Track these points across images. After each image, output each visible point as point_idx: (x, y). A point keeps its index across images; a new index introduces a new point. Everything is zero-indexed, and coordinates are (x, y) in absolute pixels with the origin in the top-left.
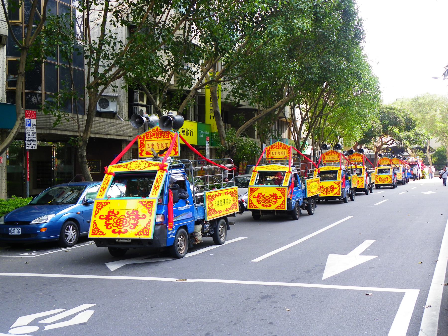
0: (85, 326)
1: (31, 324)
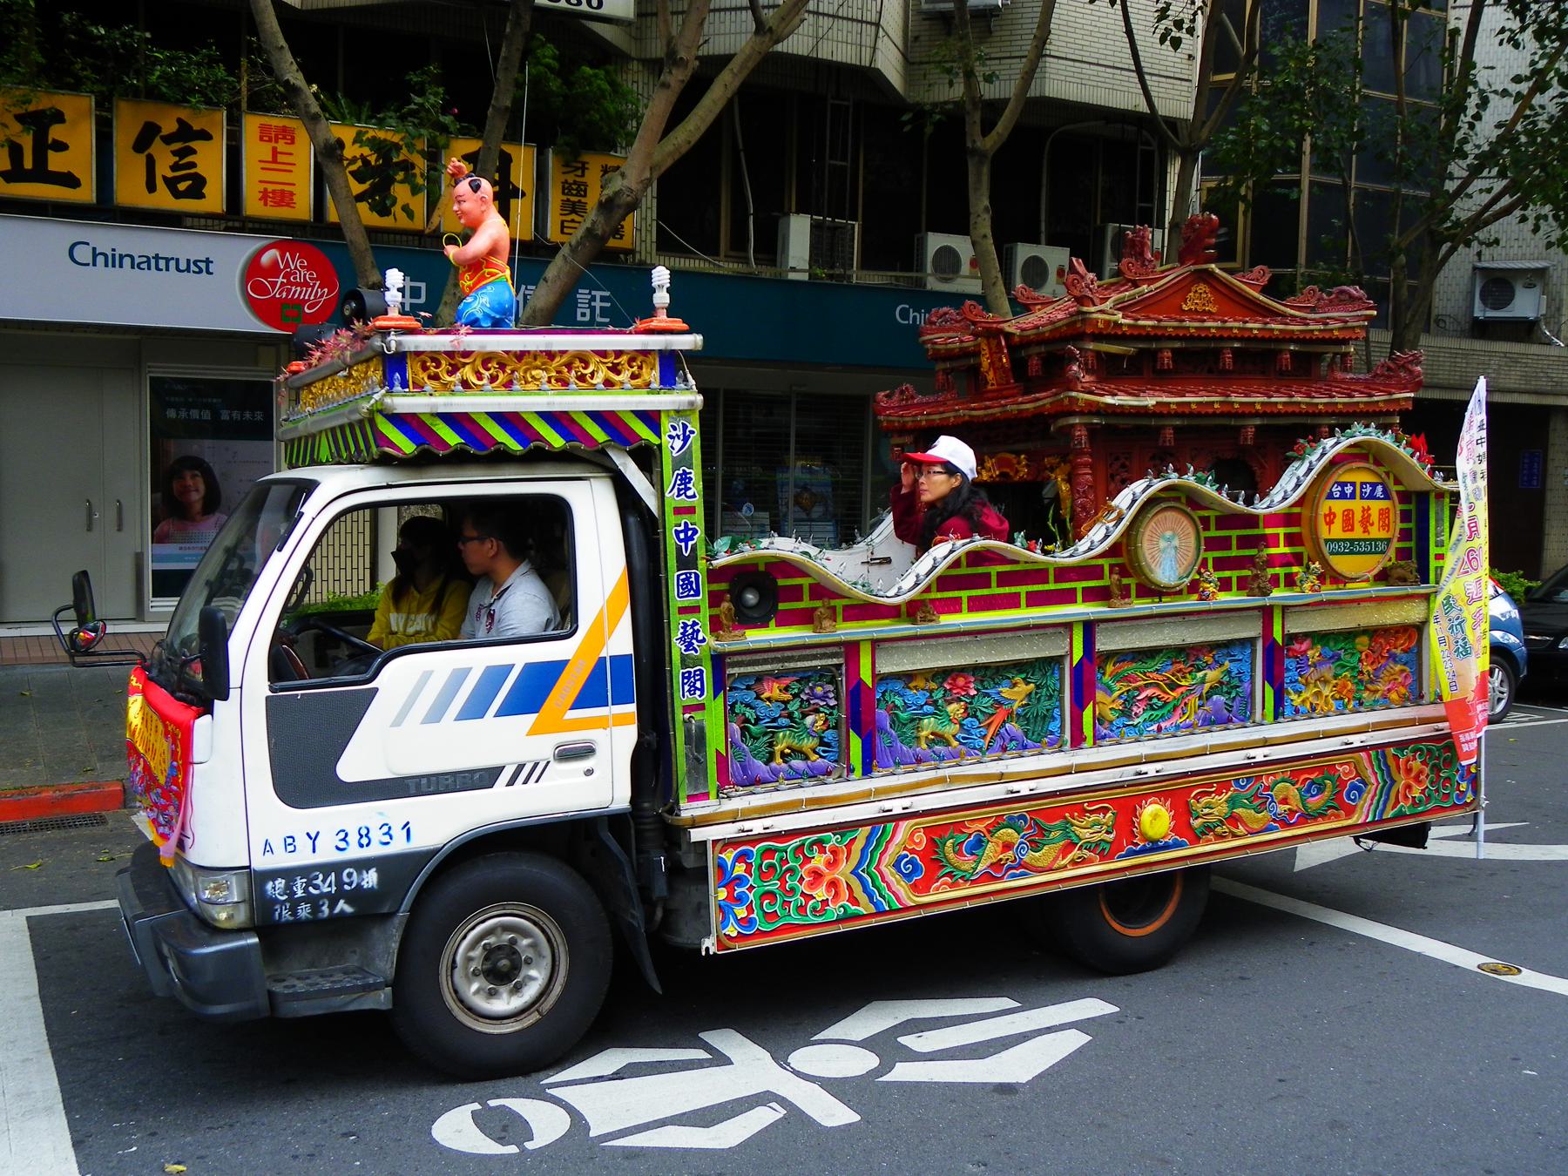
0: (1006, 1100)
1: (867, 1044)
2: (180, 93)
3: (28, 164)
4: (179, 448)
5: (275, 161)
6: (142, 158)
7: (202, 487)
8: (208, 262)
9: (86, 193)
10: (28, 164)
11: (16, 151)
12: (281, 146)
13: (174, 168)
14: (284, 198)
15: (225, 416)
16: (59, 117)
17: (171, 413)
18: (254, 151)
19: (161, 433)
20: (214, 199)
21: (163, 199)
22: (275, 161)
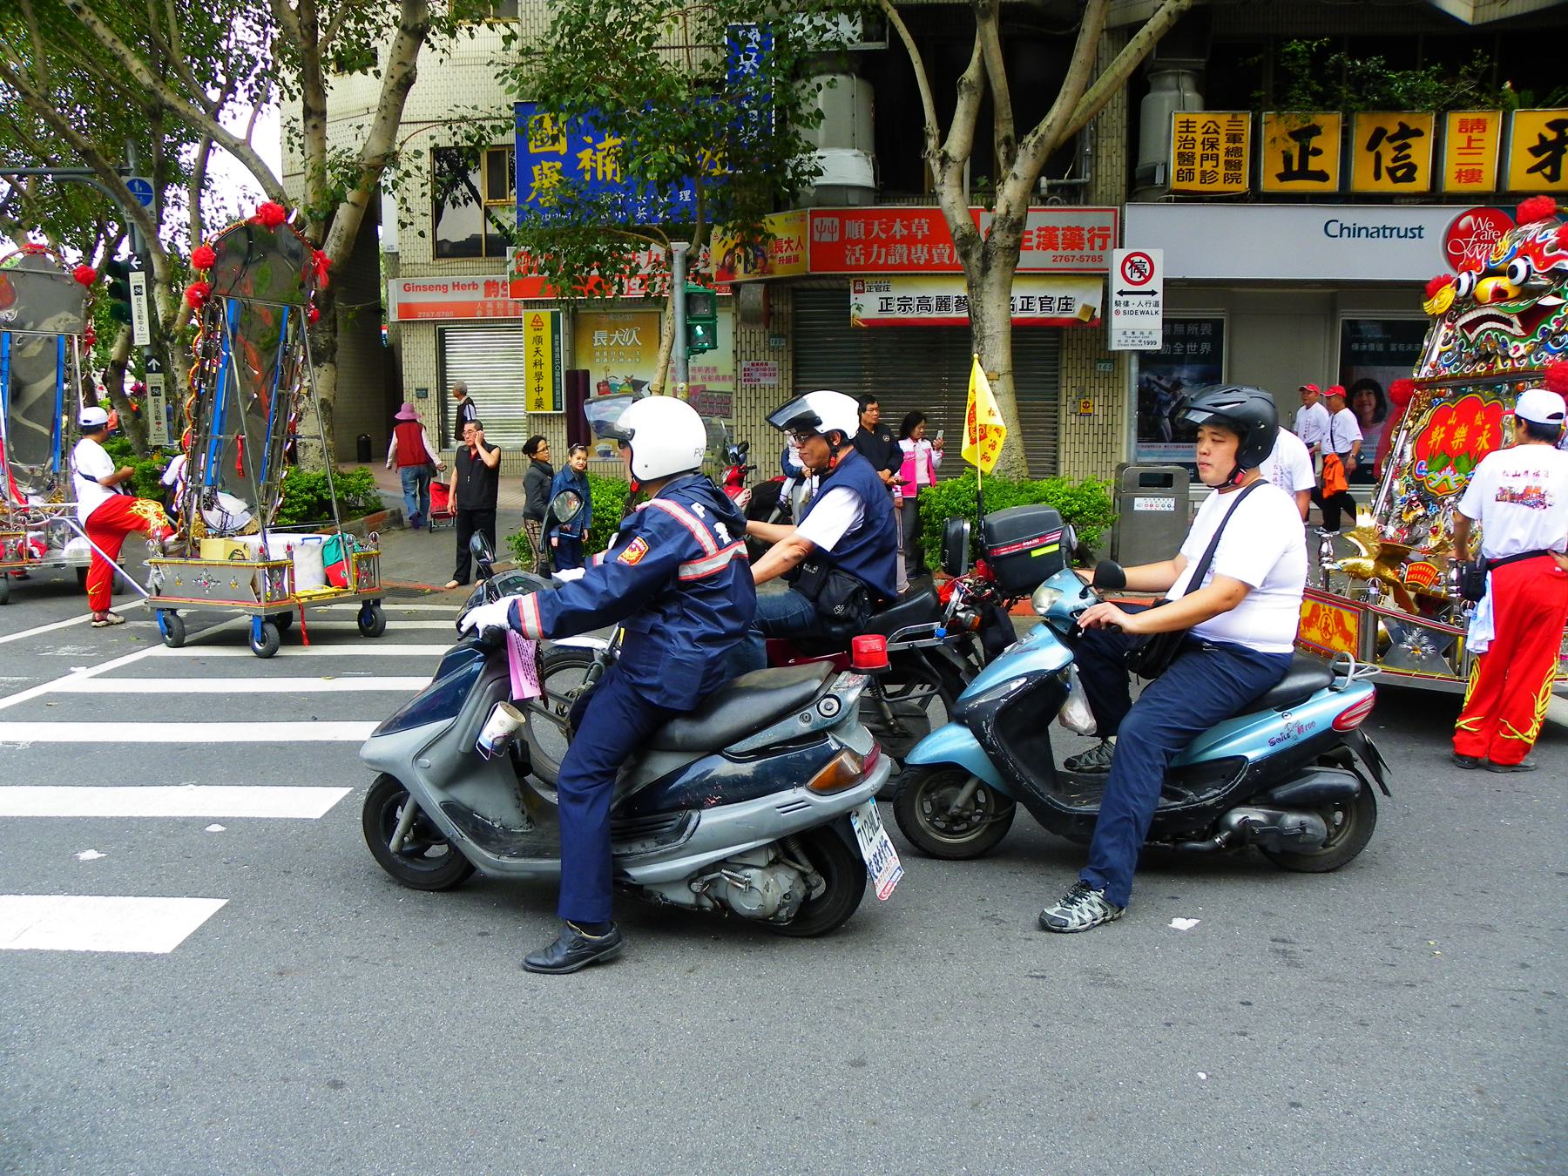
2: (1414, 100)
3: (1295, 167)
4: (1362, 372)
5: (1469, 147)
6: (1372, 155)
7: (1374, 402)
8: (1420, 228)
9: (1332, 185)
10: (1295, 167)
11: (1288, 160)
12: (1475, 135)
13: (1395, 160)
14: (1474, 176)
15: (1393, 349)
16: (1315, 130)
17: (1356, 347)
18: (1454, 139)
19: (1350, 360)
20: (1422, 182)
21: (1386, 185)
22: (1469, 147)
